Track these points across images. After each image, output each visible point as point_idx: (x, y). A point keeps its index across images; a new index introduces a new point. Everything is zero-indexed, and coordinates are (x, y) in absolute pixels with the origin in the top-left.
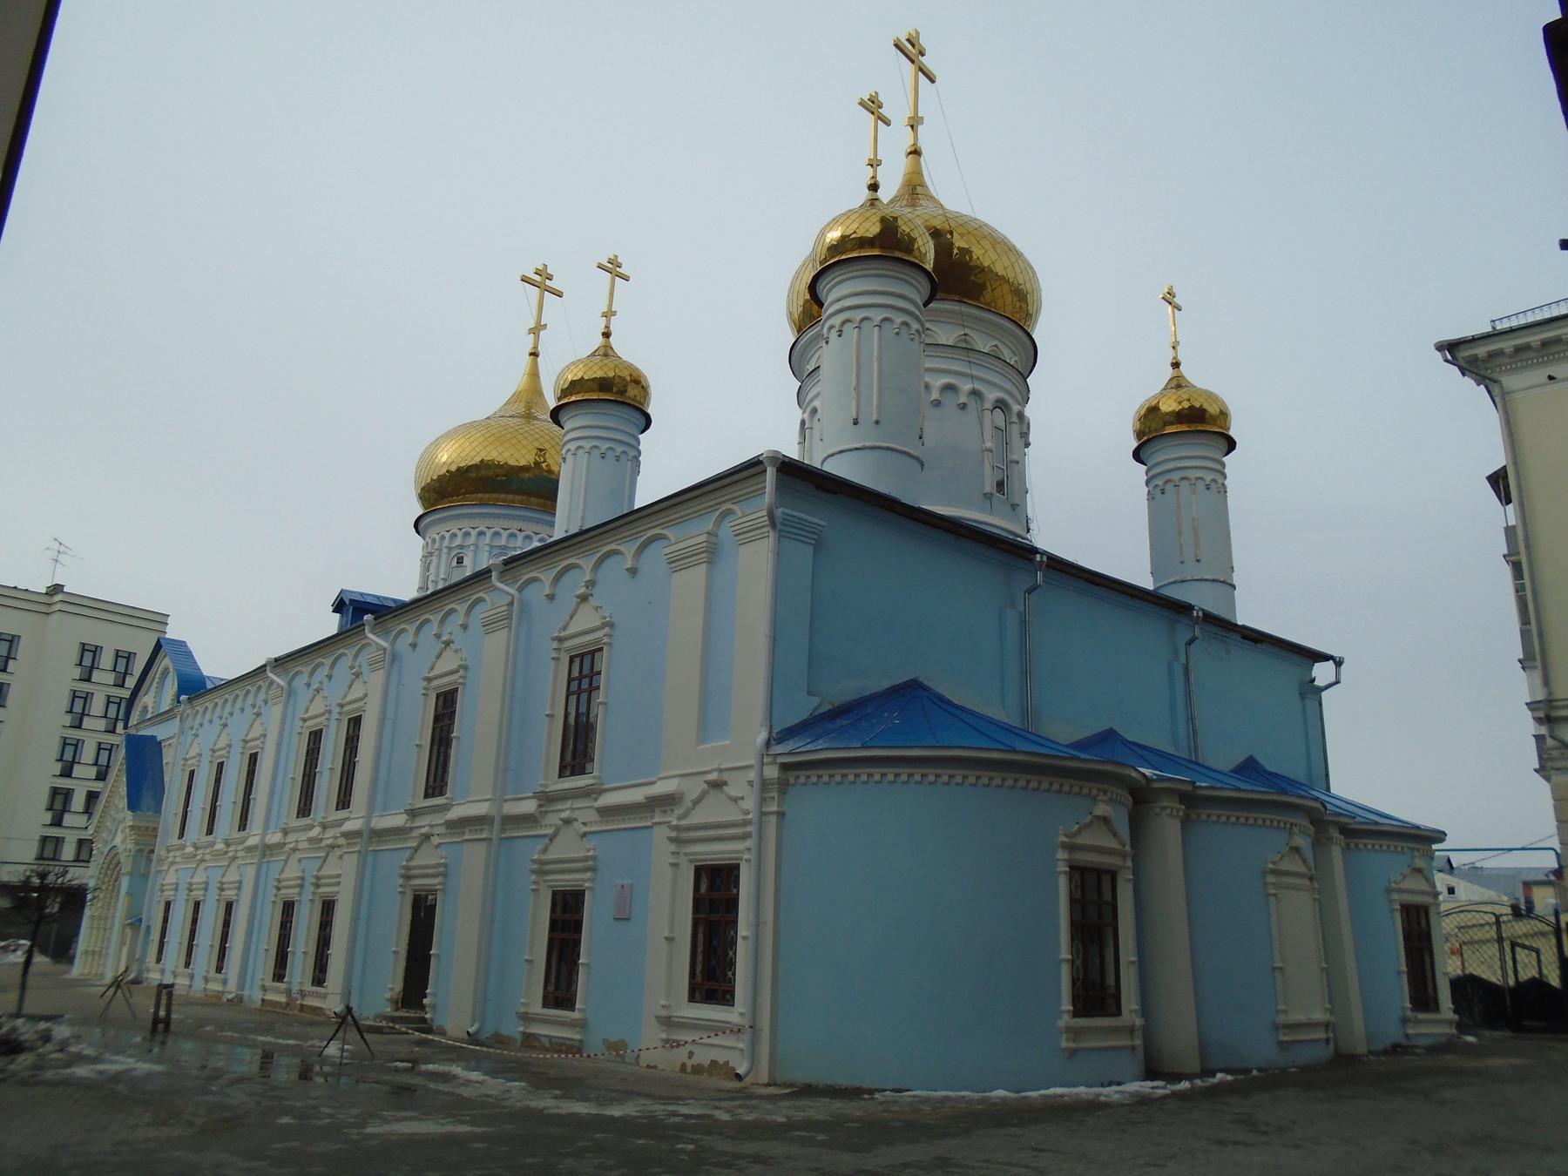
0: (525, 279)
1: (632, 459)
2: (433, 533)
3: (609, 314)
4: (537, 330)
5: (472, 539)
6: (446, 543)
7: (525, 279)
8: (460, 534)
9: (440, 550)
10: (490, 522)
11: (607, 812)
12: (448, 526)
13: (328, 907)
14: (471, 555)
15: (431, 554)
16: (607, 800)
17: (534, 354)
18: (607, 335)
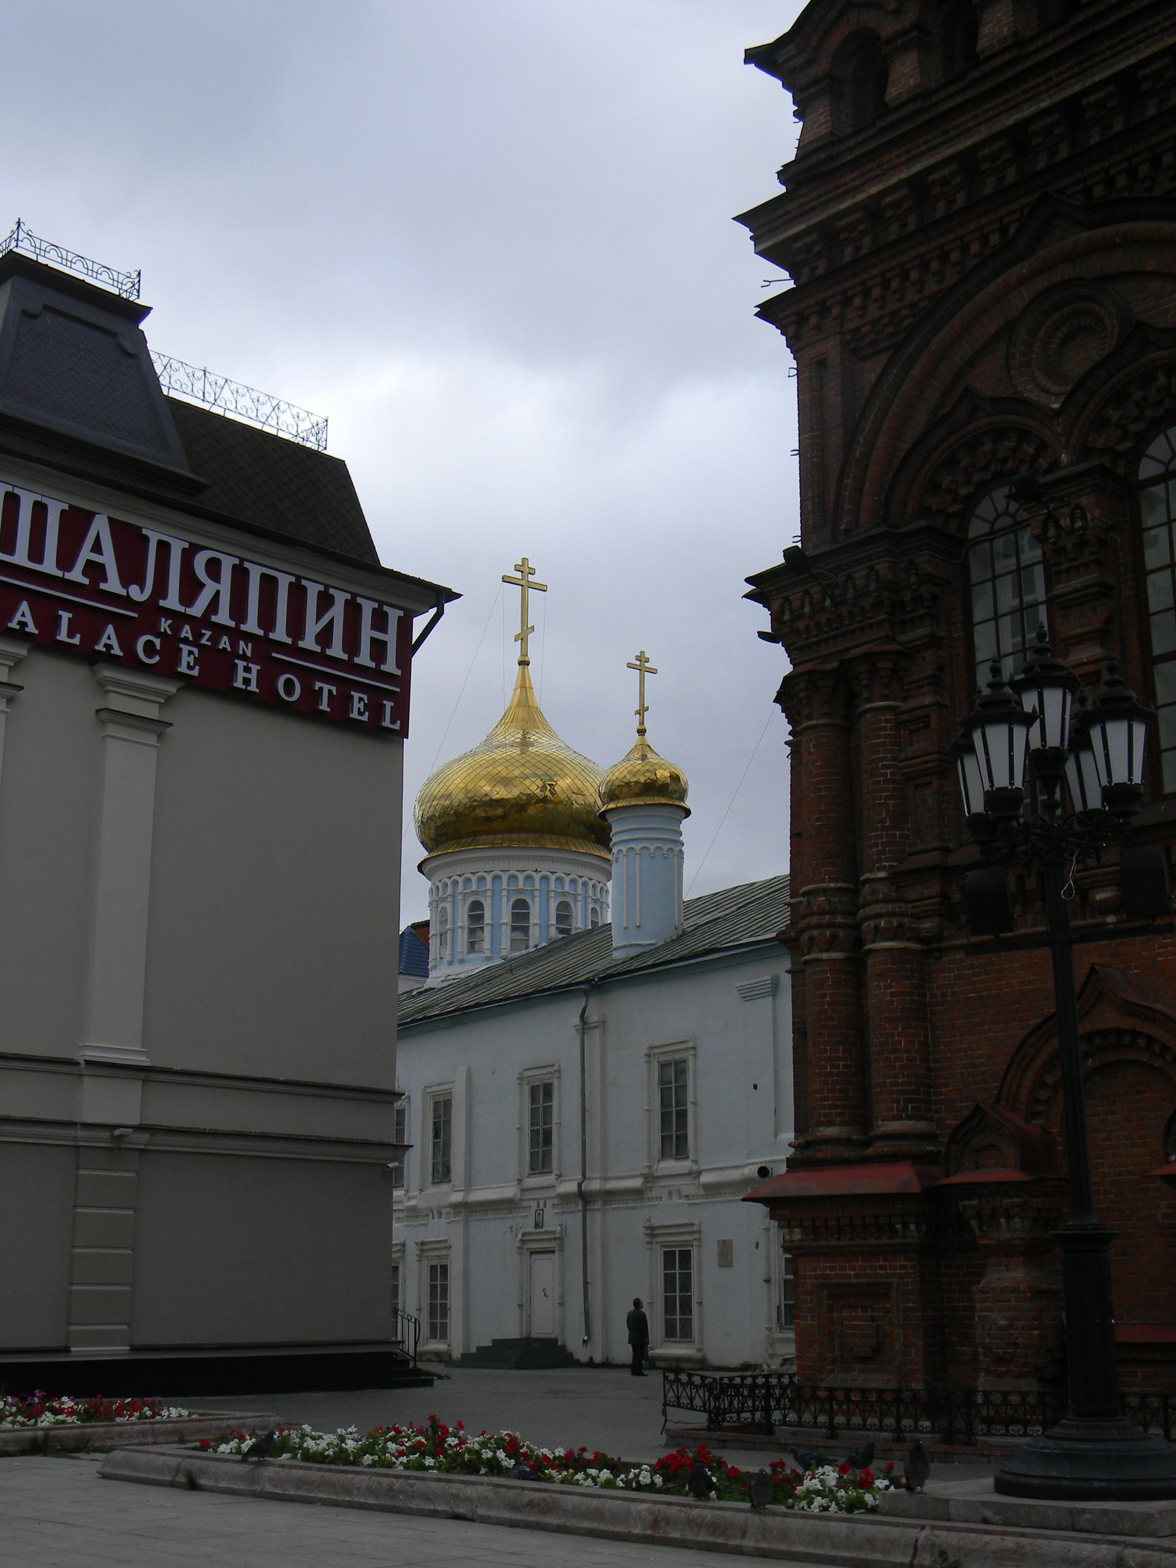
0: (505, 580)
1: (674, 851)
2: (443, 875)
3: (642, 711)
4: (522, 638)
5: (489, 885)
6: (460, 888)
7: (505, 580)
8: (474, 878)
9: (454, 896)
10: (505, 866)
11: (712, 1189)
12: (459, 869)
13: (439, 1273)
14: (489, 900)
15: (444, 899)
16: (706, 1178)
17: (524, 663)
18: (642, 732)
